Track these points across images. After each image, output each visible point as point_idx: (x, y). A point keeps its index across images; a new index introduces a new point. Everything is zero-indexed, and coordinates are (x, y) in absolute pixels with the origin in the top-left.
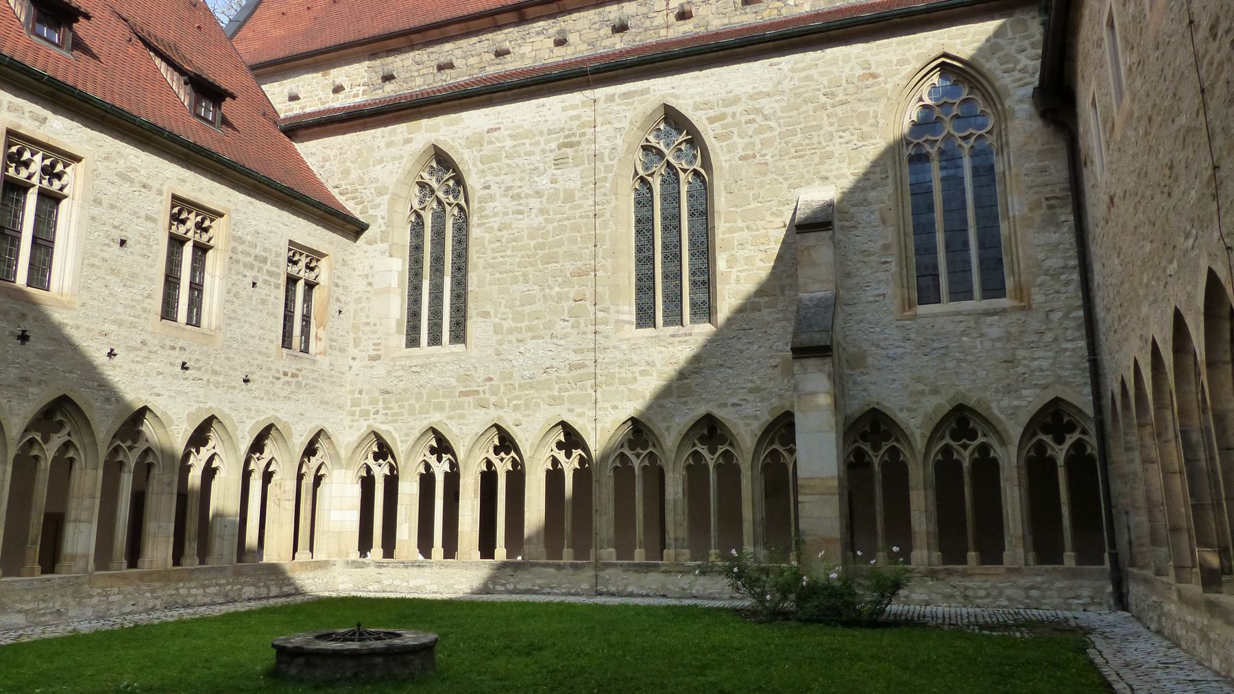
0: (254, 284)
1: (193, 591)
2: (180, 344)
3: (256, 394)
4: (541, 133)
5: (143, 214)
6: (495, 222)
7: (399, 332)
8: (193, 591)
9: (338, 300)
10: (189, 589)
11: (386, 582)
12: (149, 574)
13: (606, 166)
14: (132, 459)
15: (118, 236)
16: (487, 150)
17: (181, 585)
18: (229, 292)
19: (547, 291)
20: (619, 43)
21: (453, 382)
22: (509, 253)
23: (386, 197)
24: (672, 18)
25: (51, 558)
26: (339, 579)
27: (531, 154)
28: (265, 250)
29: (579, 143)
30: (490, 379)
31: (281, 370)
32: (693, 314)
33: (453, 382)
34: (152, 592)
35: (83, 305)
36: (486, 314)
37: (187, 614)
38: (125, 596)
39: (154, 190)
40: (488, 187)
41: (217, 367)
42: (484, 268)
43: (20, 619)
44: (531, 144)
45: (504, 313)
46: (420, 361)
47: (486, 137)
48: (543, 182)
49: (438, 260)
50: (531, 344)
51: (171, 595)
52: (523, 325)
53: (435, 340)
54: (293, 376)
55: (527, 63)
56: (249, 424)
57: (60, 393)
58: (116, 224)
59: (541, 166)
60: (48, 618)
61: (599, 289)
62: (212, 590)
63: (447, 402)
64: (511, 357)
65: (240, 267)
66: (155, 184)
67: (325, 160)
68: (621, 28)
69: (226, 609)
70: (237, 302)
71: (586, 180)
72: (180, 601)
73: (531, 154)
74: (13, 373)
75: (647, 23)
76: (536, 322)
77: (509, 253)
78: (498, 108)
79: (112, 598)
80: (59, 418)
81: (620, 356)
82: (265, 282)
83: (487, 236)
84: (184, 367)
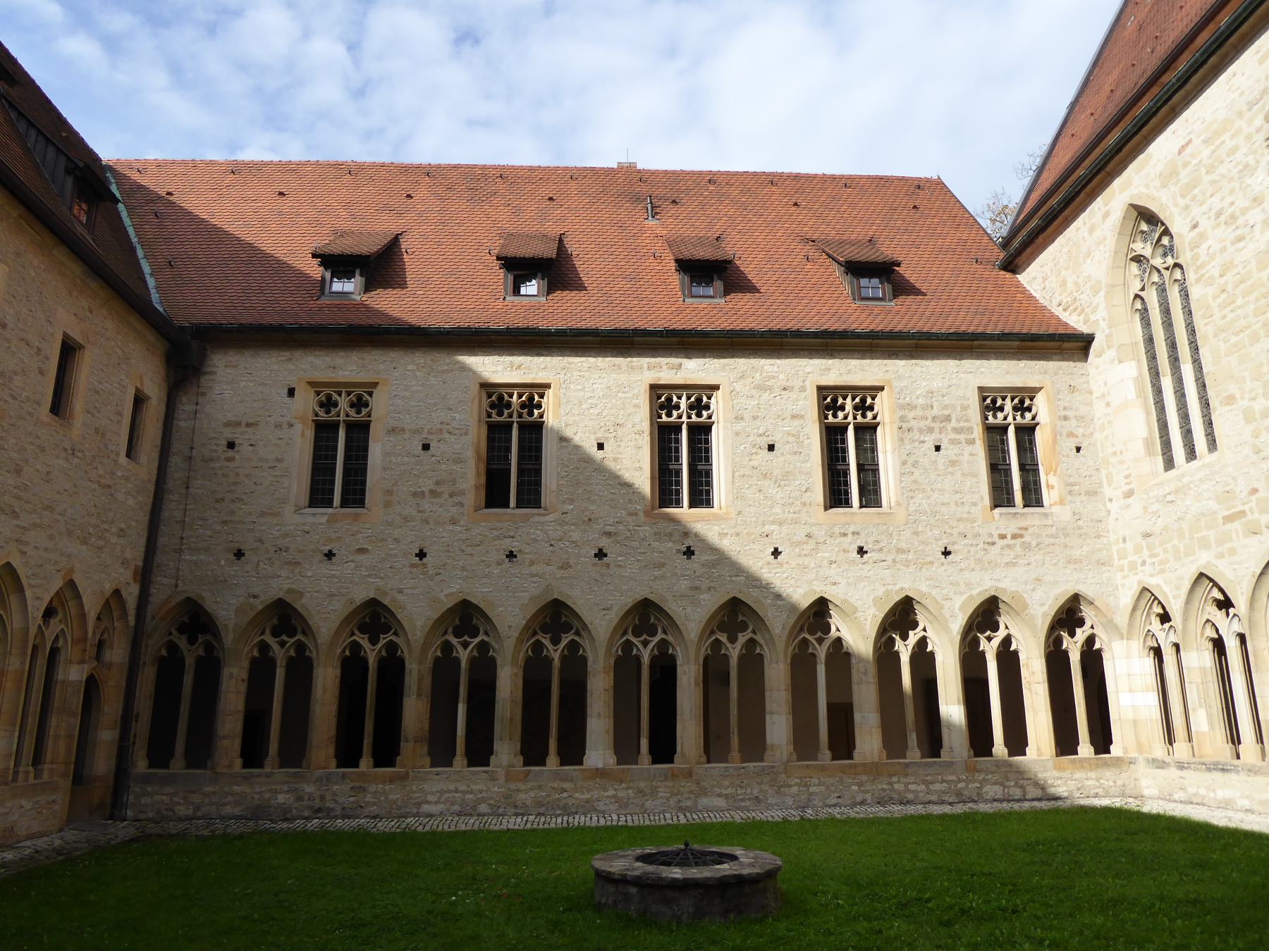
0: (938, 448)
1: (912, 787)
2: (851, 529)
3: (962, 565)
4: (1240, 114)
5: (788, 414)
8: (912, 787)
9: (1071, 435)
10: (907, 784)
11: (1191, 790)
12: (855, 766)
14: (822, 652)
15: (764, 442)
17: (895, 779)
18: (904, 463)
21: (1213, 505)
22: (1239, 302)
23: (1102, 293)
25: (755, 746)
26: (1144, 782)
27: (1232, 152)
28: (945, 407)
30: (1255, 491)
31: (995, 534)
33: (1213, 505)
34: (860, 785)
35: (740, 513)
36: (1230, 400)
37: (911, 810)
38: (827, 787)
39: (796, 389)
40: (1195, 226)
41: (903, 545)
42: (1215, 336)
43: (721, 803)
44: (1232, 137)
49: (1172, 346)
51: (883, 790)
53: (1191, 454)
54: (1014, 537)
56: (958, 601)
57: (729, 597)
58: (761, 431)
59: (1251, 160)
60: (747, 803)
62: (937, 787)
65: (916, 434)
66: (797, 383)
67: (1045, 279)
69: (959, 809)
70: (917, 472)
72: (895, 796)
73: (1232, 152)
74: (684, 584)
77: (1239, 302)
78: (1186, 115)
79: (811, 789)
80: (740, 618)
82: (952, 442)
83: (1210, 291)
84: (861, 551)
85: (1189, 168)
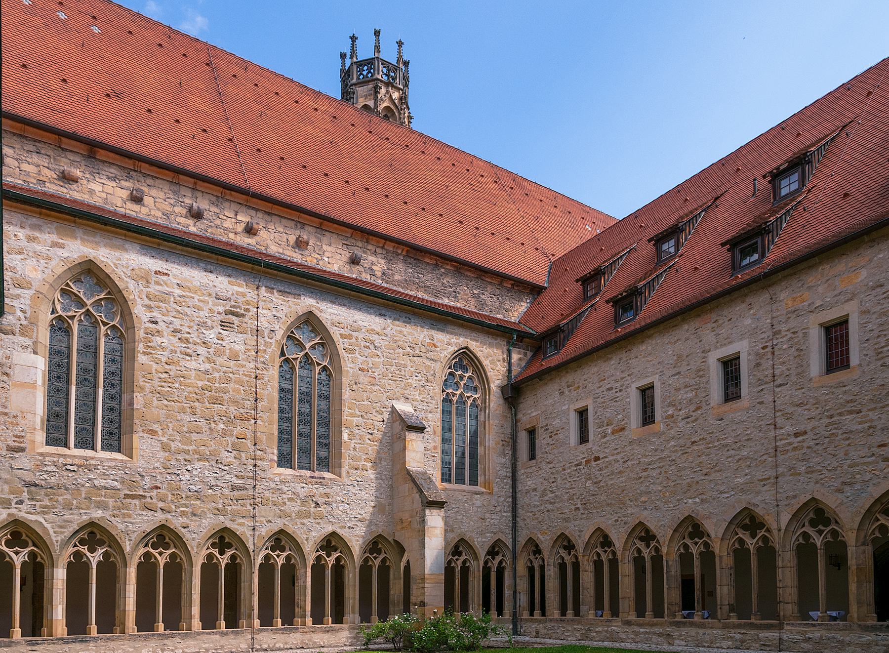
6: (164, 356)
7: (42, 429)
13: (266, 342)
16: (154, 289)
19: (213, 425)
20: (192, 227)
24: (240, 228)
29: (243, 316)
30: (157, 488)
32: (319, 465)
36: (153, 432)
45: (171, 435)
46: (82, 462)
47: (154, 278)
48: (211, 335)
50: (198, 465)
52: (191, 448)
55: (84, 197)
59: (209, 323)
61: (258, 434)
63: (111, 502)
64: (179, 472)
68: (197, 215)
71: (249, 347)
75: (218, 222)
76: (203, 448)
81: (273, 485)
85: (158, 287)
